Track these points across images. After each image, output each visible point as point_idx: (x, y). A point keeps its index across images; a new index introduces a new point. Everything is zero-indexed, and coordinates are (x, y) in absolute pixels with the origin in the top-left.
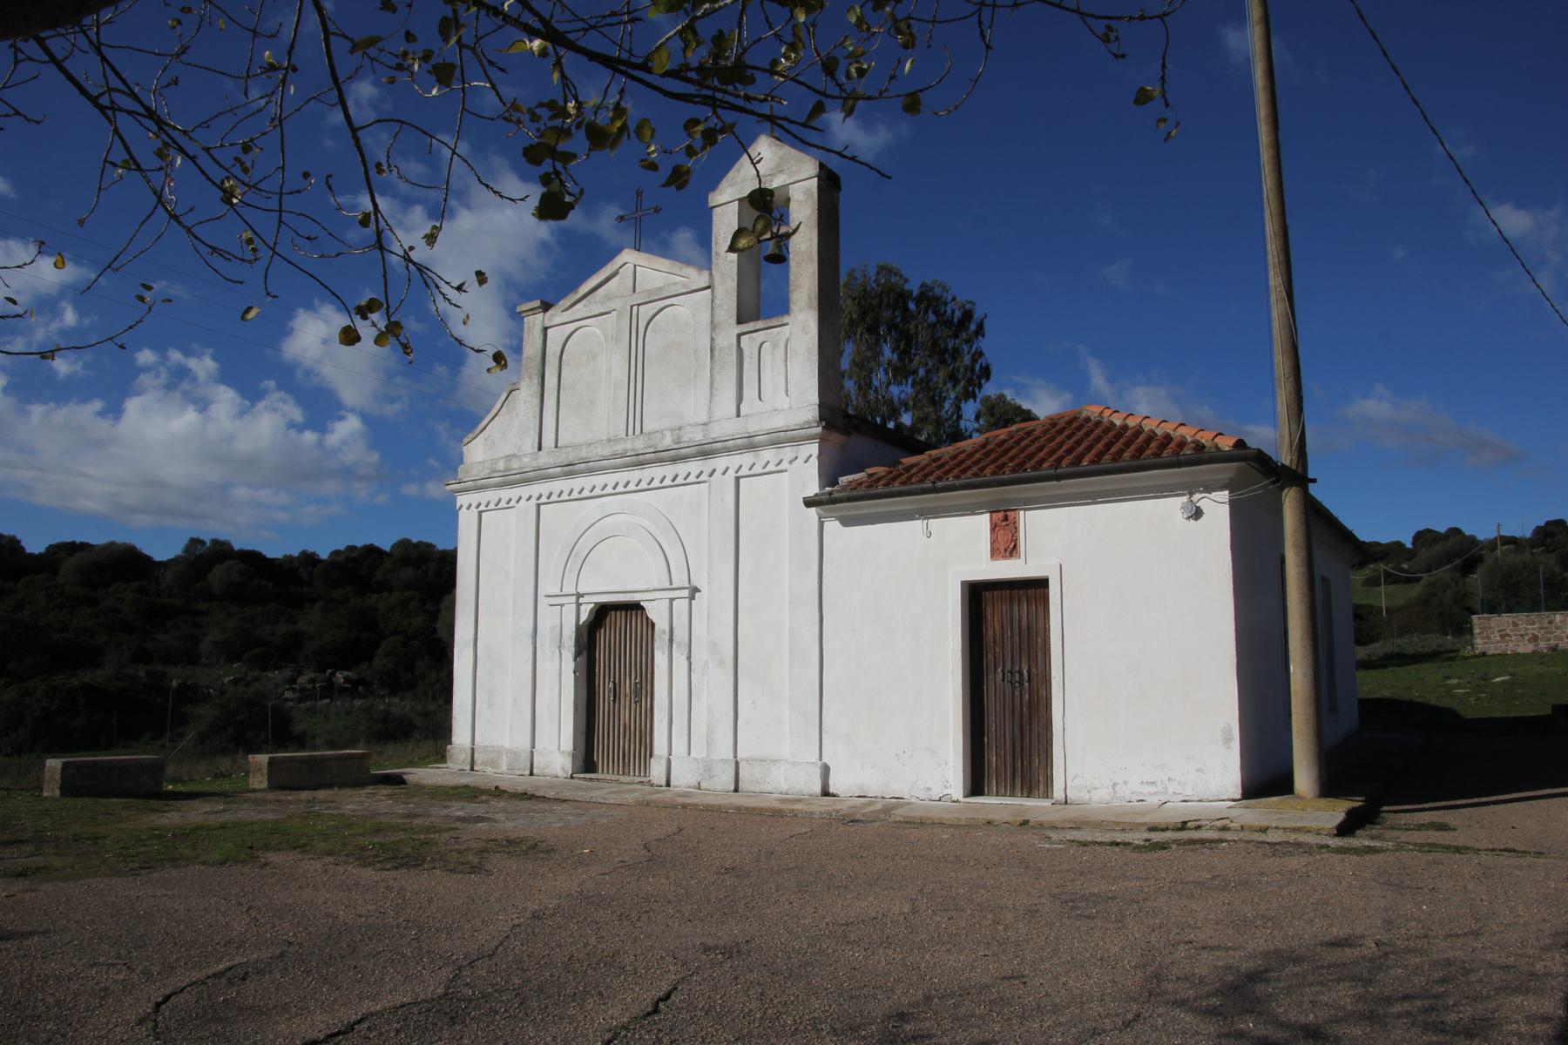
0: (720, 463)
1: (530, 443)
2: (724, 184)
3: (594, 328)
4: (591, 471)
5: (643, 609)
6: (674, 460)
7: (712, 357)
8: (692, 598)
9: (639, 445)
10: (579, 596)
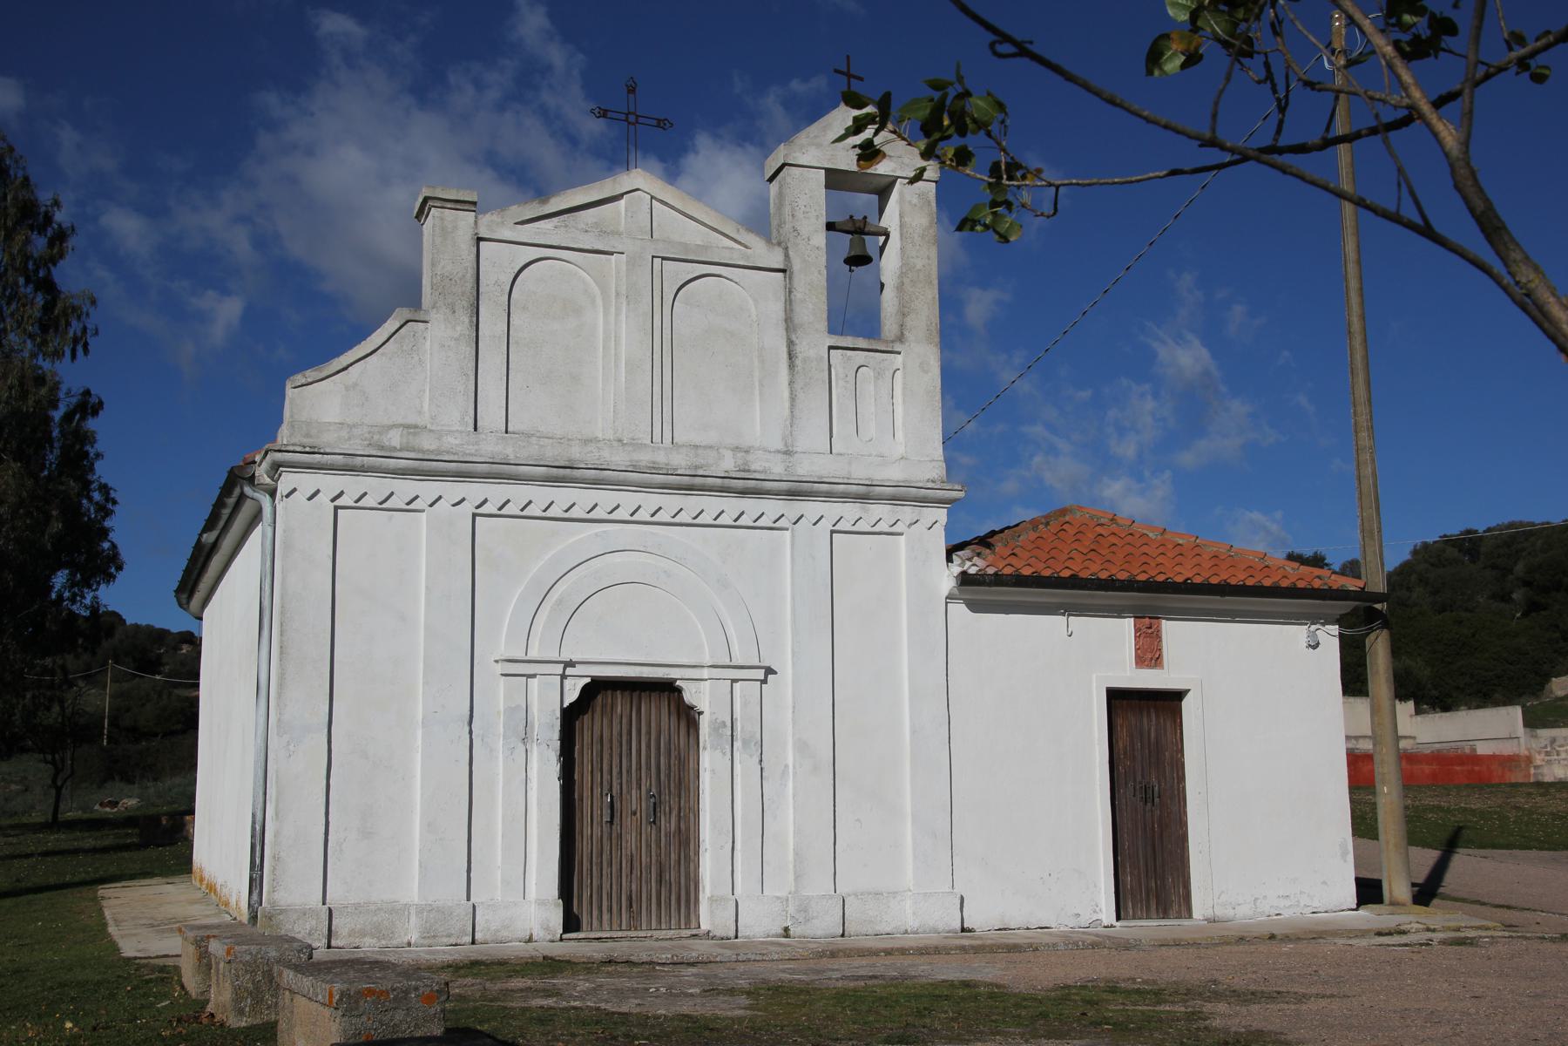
0: (812, 508)
1: (455, 415)
2: (802, 138)
3: (576, 273)
4: (596, 483)
5: (679, 691)
6: (744, 493)
7: (792, 366)
8: (764, 681)
9: (680, 461)
10: (570, 664)
